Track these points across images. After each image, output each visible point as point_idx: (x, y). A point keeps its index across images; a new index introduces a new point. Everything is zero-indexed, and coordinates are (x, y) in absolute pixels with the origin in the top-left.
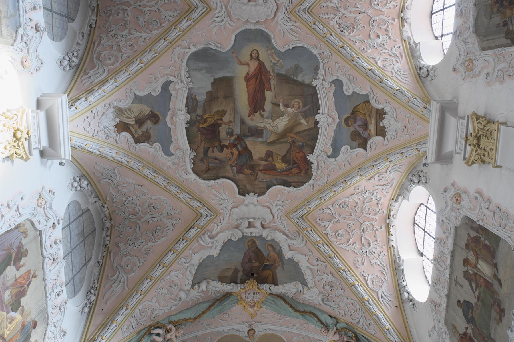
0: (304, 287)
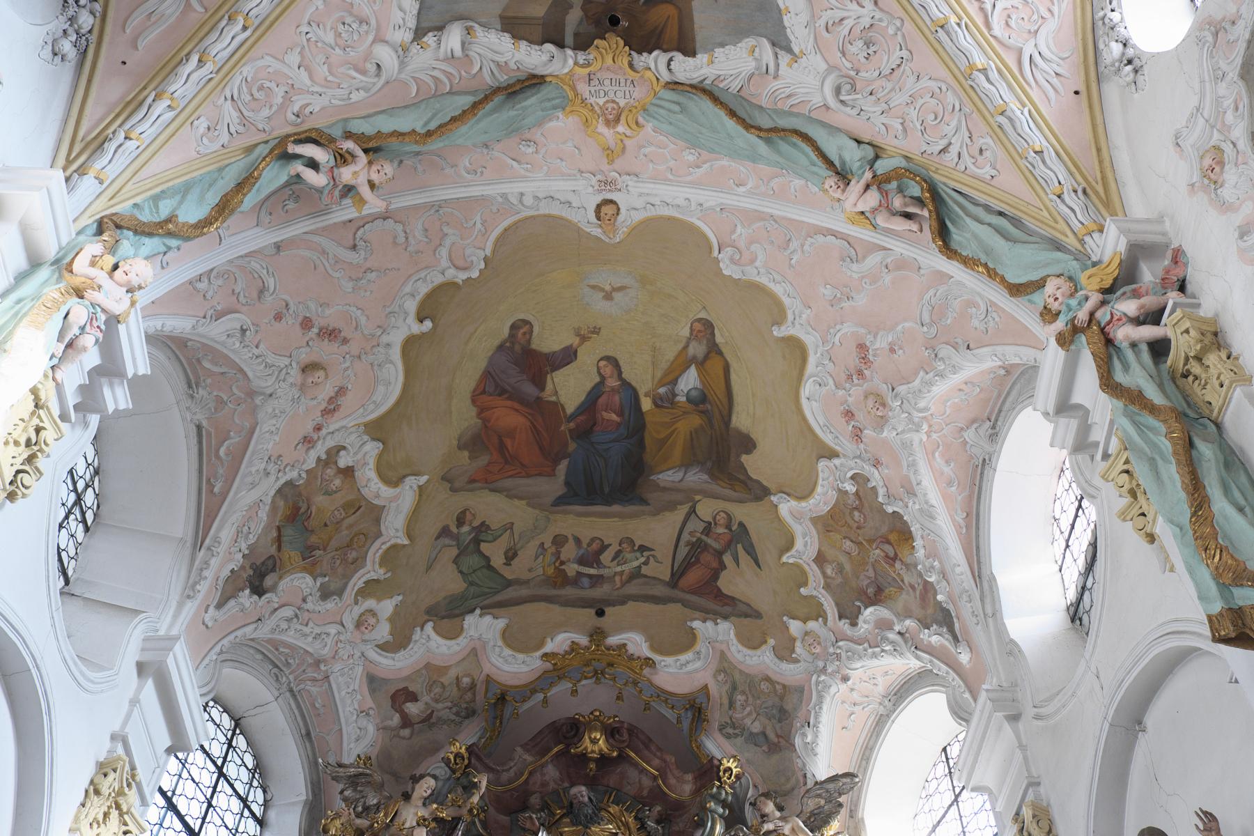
0: (781, 53)
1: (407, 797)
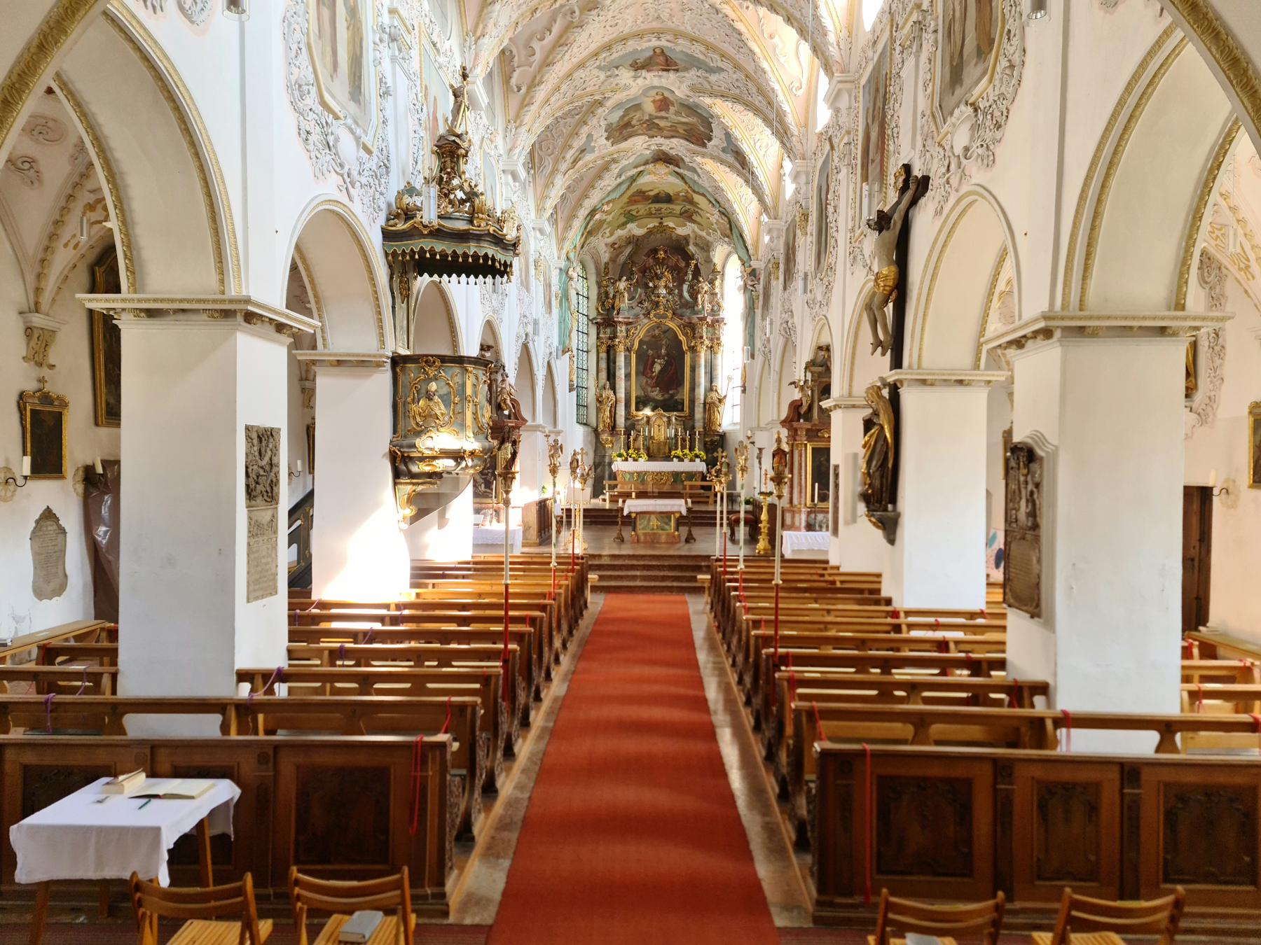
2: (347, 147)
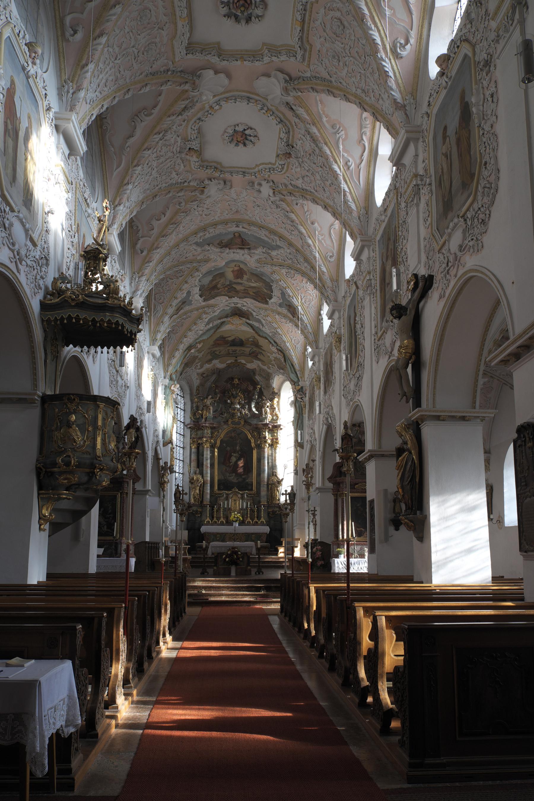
1: (207, 398)
2: (18, 230)
